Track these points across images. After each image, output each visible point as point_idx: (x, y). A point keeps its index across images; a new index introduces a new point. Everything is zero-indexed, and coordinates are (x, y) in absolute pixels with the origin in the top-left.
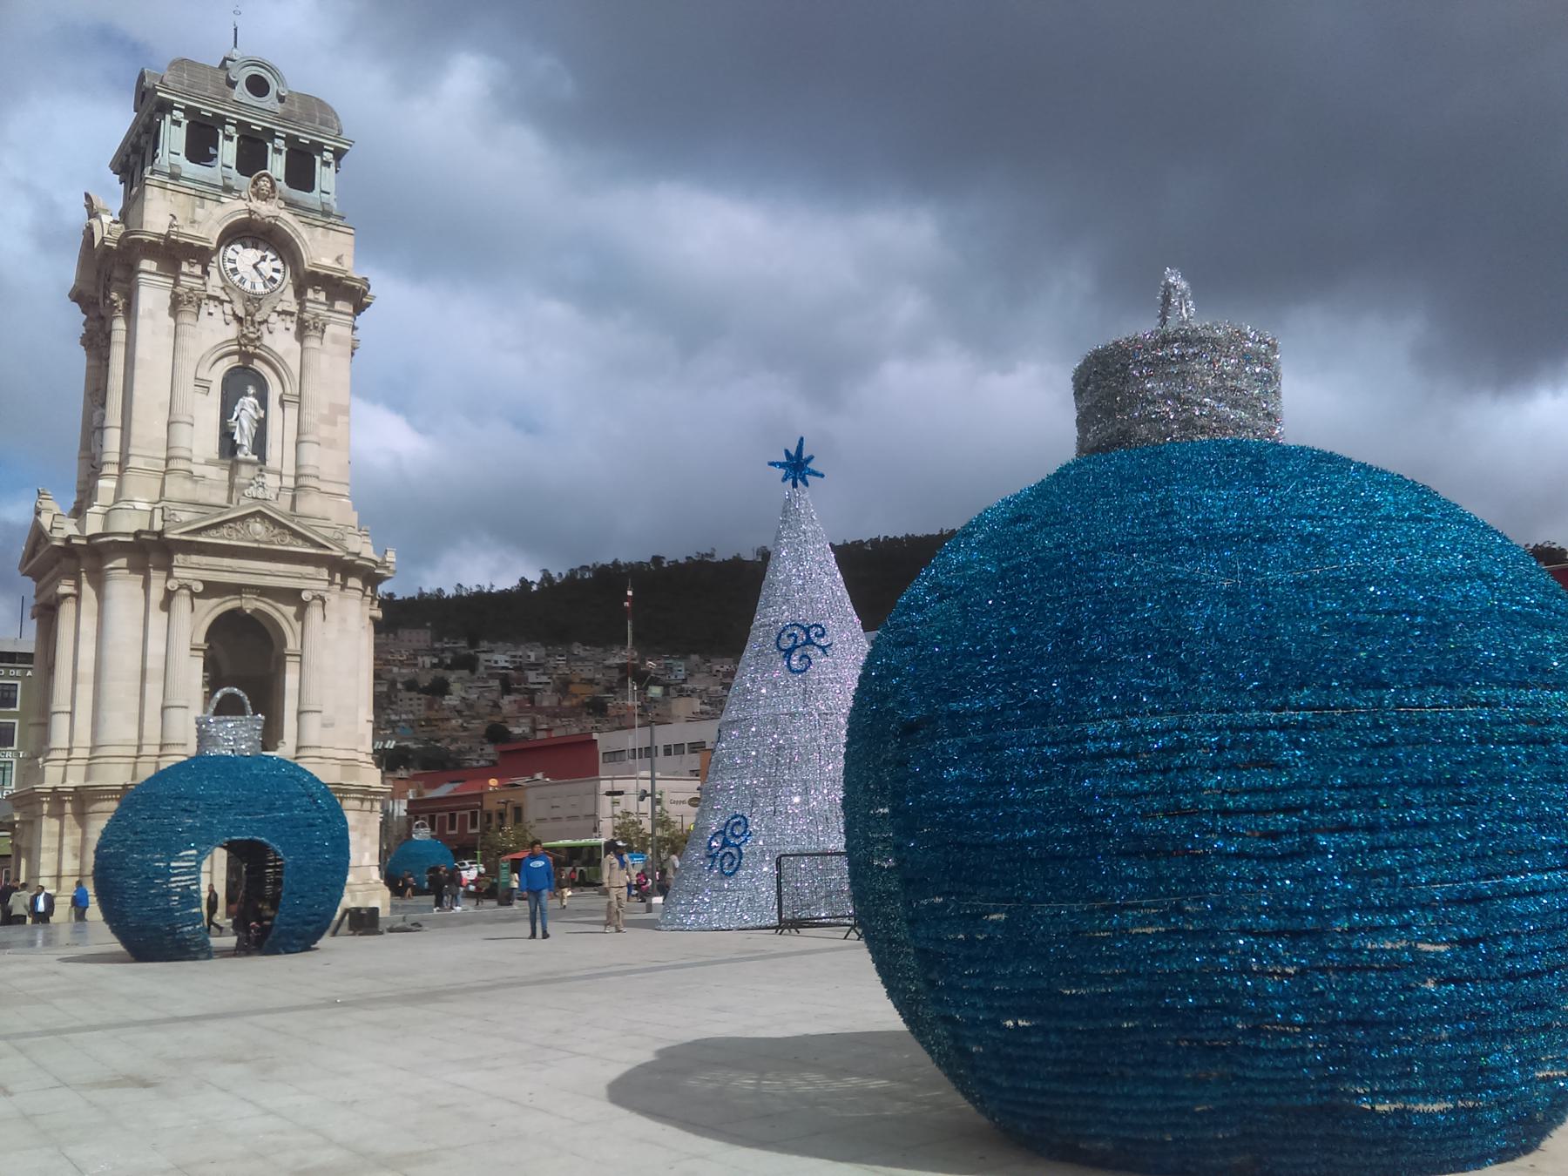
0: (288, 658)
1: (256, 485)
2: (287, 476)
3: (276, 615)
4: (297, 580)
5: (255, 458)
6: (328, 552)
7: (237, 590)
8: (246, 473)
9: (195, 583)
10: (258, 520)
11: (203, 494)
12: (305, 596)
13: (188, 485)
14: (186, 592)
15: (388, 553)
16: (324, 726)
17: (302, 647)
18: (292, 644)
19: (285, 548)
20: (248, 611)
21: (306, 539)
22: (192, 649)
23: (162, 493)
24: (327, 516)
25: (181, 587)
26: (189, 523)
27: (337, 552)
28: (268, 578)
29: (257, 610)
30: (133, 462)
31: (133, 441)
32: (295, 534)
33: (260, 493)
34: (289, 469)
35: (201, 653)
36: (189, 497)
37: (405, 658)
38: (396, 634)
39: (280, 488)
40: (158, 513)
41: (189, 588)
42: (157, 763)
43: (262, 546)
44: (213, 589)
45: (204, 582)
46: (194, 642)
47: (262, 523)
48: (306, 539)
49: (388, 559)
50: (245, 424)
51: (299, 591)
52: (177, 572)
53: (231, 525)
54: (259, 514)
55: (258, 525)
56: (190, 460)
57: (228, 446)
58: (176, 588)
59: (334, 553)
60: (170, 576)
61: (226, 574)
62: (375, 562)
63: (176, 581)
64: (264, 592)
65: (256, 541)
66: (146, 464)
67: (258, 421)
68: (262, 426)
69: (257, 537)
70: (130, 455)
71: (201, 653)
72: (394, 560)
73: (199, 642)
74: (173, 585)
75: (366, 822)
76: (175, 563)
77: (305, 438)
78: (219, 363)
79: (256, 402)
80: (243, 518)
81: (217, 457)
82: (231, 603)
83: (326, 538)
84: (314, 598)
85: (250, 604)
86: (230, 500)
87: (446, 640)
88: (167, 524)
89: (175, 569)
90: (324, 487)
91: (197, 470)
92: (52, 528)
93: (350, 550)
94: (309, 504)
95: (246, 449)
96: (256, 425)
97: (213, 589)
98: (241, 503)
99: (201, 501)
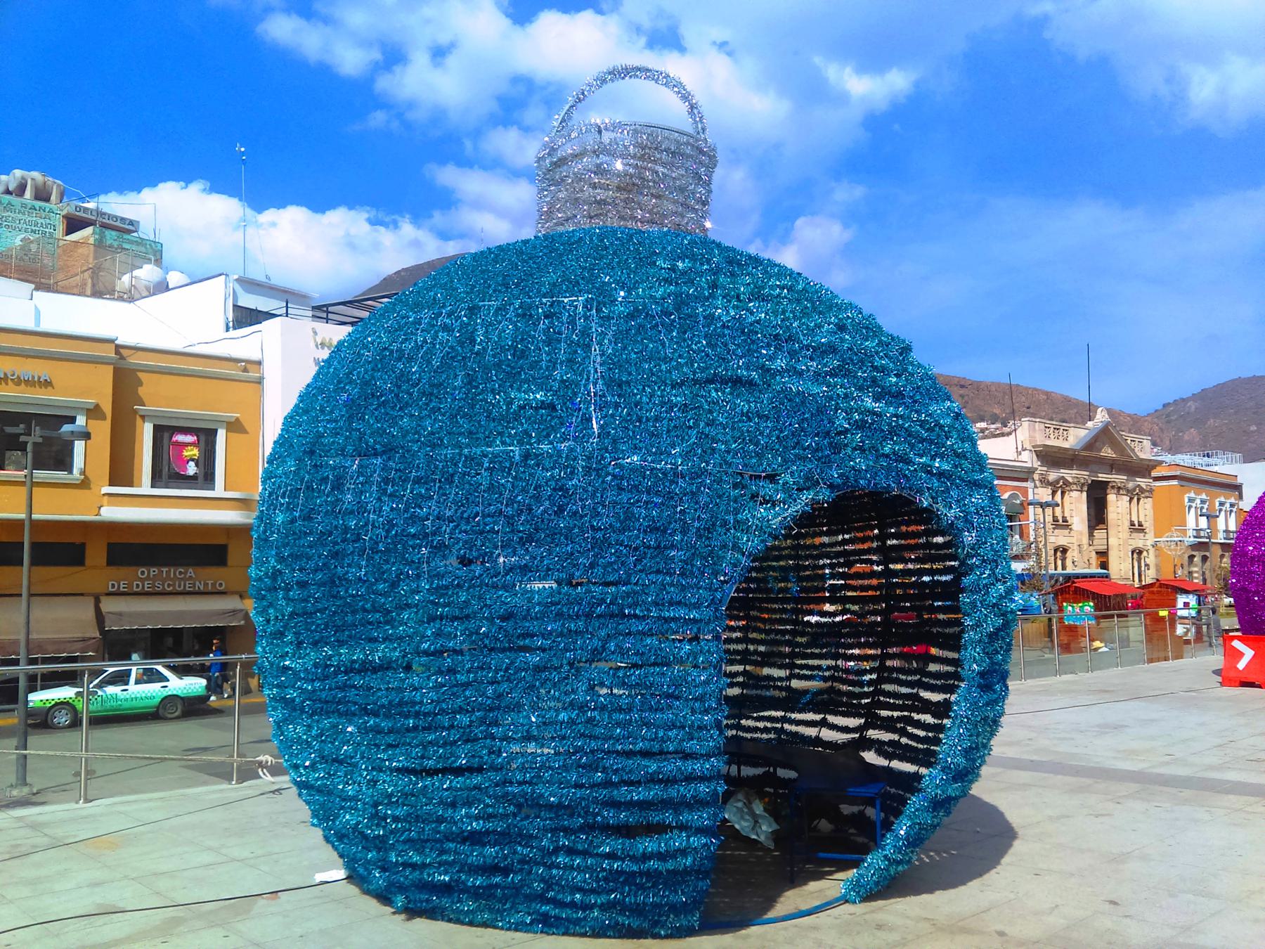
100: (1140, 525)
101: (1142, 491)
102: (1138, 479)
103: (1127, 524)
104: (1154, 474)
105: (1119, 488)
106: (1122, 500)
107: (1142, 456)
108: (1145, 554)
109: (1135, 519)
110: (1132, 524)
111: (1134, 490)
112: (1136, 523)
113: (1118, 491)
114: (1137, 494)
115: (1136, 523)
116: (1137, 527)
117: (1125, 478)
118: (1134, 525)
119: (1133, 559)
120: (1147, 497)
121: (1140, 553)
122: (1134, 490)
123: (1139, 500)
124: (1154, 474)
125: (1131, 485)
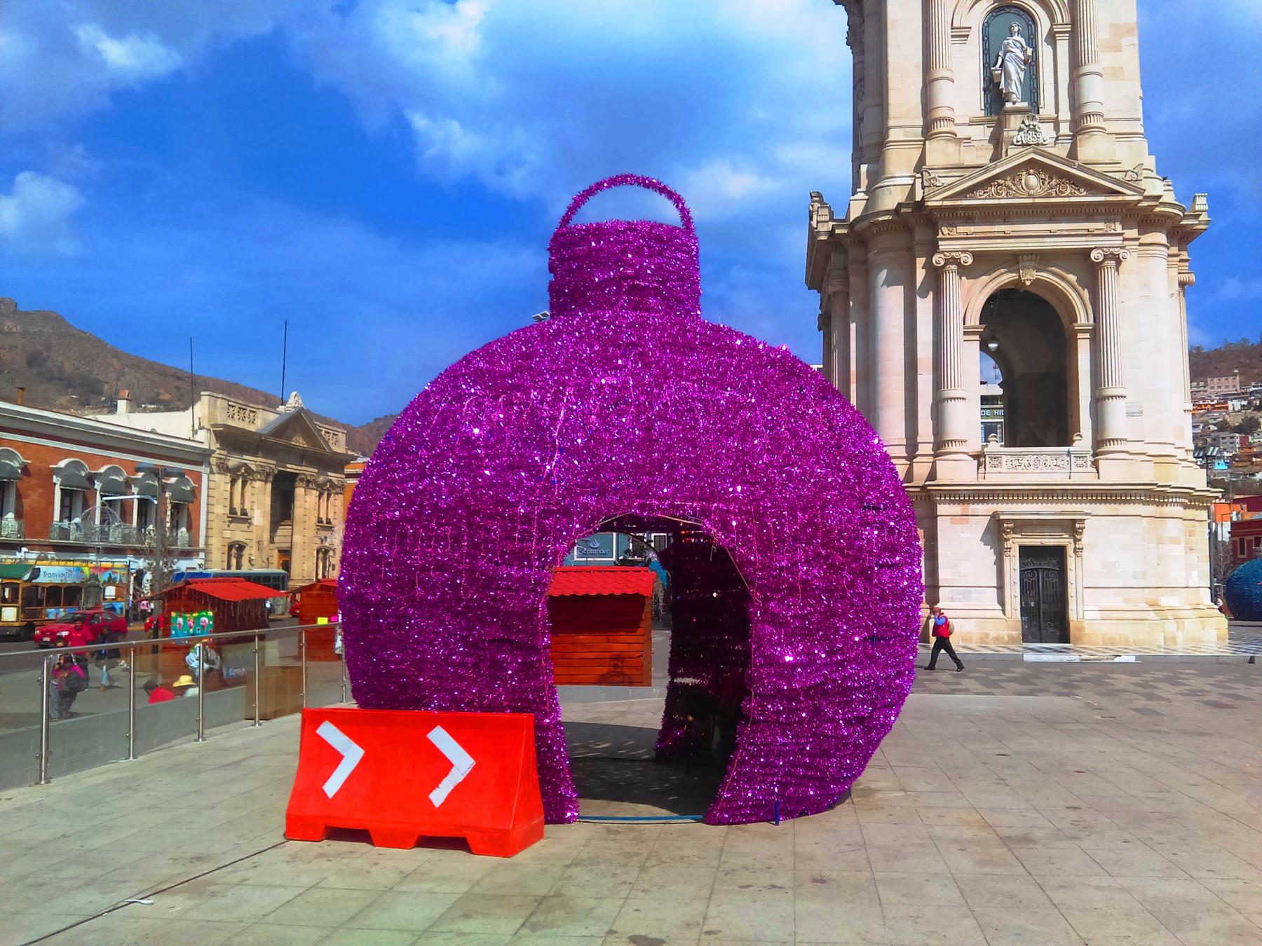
0: (1079, 336)
1: (1026, 129)
2: (1064, 121)
3: (1062, 285)
4: (1084, 239)
5: (1025, 104)
6: (1120, 198)
7: (1013, 259)
8: (1015, 122)
9: (962, 255)
10: (1032, 171)
11: (969, 158)
12: (1093, 254)
13: (951, 147)
14: (954, 267)
15: (1197, 198)
16: (1130, 414)
17: (1094, 321)
18: (1083, 318)
19: (1067, 200)
20: (1028, 283)
21: (1092, 188)
22: (965, 333)
23: (922, 160)
24: (1117, 160)
25: (947, 262)
26: (951, 186)
27: (1131, 197)
28: (1048, 240)
29: (1036, 282)
30: (894, 135)
31: (892, 111)
32: (1077, 182)
33: (1030, 138)
34: (1065, 114)
35: (977, 337)
36: (954, 160)
37: (1215, 402)
38: (1206, 382)
39: (1057, 139)
40: (919, 182)
41: (956, 261)
42: (934, 463)
43: (1037, 200)
44: (984, 262)
45: (976, 255)
46: (968, 324)
47: (1037, 174)
48: (1092, 188)
49: (1197, 208)
50: (1012, 68)
51: (1086, 253)
52: (943, 245)
53: (1001, 181)
54: (1031, 165)
55: (1032, 177)
56: (951, 120)
57: (995, 96)
58: (942, 263)
59: (1127, 198)
60: (934, 248)
61: (999, 241)
62: (1183, 210)
63: (942, 256)
64: (1043, 258)
65: (1030, 196)
66: (905, 136)
67: (1025, 62)
68: (1032, 65)
69: (1032, 192)
70: (889, 128)
71: (977, 337)
72: (1206, 207)
73: (973, 324)
74: (938, 259)
75: (1191, 533)
76: (940, 236)
77: (1086, 69)
78: (976, 5)
79: (1022, 40)
80: (1014, 172)
81: (982, 114)
82: (1005, 278)
83: (1116, 182)
84: (1106, 257)
85: (1029, 276)
86: (996, 157)
87: (1253, 384)
88: (926, 189)
89: (940, 243)
90: (1111, 127)
91: (961, 132)
92: (818, 222)
93: (1146, 194)
94: (1093, 149)
95: (1014, 96)
96: (1023, 67)
97: (984, 262)
98: (1011, 152)
99: (966, 164)
100: (329, 522)
101: (333, 485)
102: (329, 474)
103: (314, 520)
104: (347, 471)
105: (308, 482)
106: (311, 494)
107: (336, 449)
108: (331, 553)
109: (323, 515)
110: (320, 521)
111: (325, 484)
112: (325, 521)
113: (307, 485)
114: (328, 489)
115: (325, 521)
116: (325, 524)
117: (316, 471)
118: (322, 522)
119: (317, 559)
120: (338, 493)
121: (326, 552)
122: (325, 484)
123: (329, 496)
124: (347, 471)
125: (321, 479)
